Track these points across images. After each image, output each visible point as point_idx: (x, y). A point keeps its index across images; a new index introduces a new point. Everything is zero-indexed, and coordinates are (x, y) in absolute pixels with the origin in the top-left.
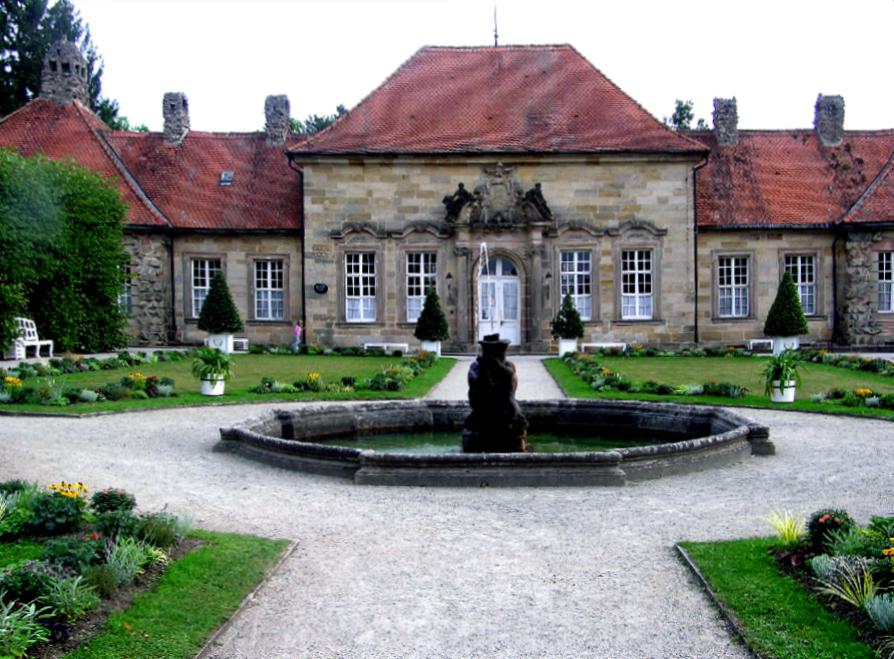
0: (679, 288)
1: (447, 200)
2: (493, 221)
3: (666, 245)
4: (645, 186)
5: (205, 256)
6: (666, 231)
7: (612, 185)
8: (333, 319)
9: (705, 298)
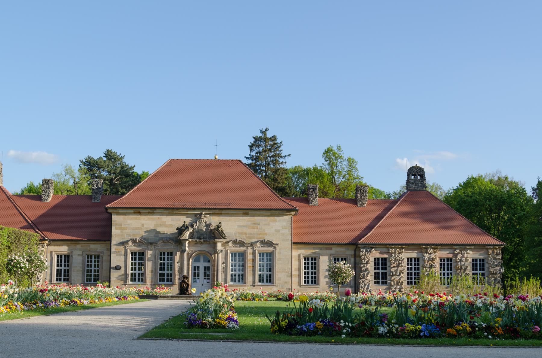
7: (255, 224)
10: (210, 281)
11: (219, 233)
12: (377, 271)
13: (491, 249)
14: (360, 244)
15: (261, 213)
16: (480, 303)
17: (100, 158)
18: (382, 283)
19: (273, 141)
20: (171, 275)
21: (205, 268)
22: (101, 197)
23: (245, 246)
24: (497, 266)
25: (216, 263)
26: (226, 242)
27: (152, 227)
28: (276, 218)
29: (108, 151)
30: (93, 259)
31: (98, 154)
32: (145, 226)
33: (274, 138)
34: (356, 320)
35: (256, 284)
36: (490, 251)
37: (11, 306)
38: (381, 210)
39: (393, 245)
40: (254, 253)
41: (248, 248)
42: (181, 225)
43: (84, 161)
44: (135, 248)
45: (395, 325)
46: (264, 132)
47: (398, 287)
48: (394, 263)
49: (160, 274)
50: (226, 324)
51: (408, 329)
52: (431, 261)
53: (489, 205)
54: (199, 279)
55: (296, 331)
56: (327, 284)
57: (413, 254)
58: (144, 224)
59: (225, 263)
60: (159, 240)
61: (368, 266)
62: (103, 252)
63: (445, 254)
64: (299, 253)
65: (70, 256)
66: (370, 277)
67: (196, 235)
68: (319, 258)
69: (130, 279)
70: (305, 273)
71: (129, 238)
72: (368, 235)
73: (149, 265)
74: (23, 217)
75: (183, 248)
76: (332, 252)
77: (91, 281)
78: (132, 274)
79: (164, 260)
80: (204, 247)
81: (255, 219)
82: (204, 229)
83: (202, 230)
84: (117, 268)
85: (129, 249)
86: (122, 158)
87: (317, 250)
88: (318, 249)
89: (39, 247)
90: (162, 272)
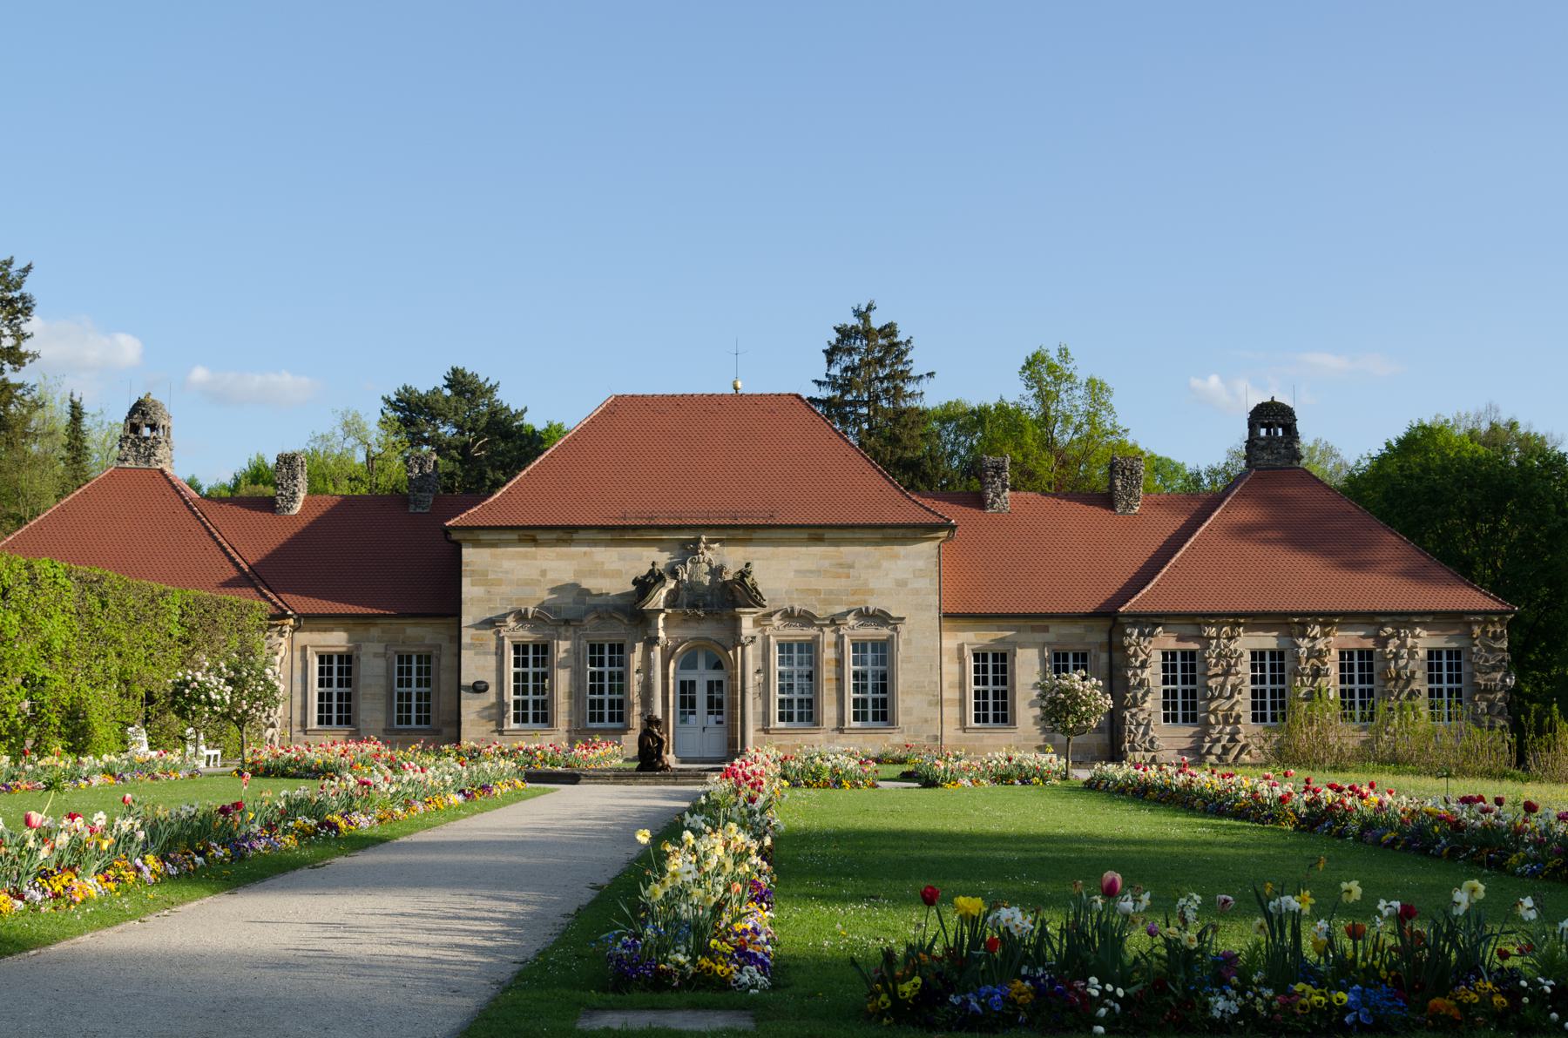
7: (841, 565)
10: (724, 718)
11: (746, 590)
12: (1170, 687)
13: (1477, 623)
14: (1123, 615)
15: (857, 536)
16: (1529, 909)
17: (436, 391)
18: (1185, 720)
19: (886, 336)
20: (621, 703)
21: (710, 684)
22: (431, 500)
23: (816, 625)
24: (1494, 668)
25: (739, 671)
26: (764, 616)
27: (568, 578)
28: (897, 549)
29: (455, 371)
30: (414, 666)
31: (429, 380)
32: (550, 576)
33: (889, 330)
34: (1137, 975)
35: (846, 726)
36: (1477, 630)
37: (123, 873)
38: (1180, 521)
39: (1212, 615)
40: (839, 644)
41: (825, 629)
42: (645, 572)
43: (394, 398)
44: (525, 635)
45: (1261, 990)
46: (863, 315)
47: (1228, 729)
48: (1216, 665)
49: (592, 702)
50: (731, 972)
51: (1304, 1001)
52: (1315, 657)
53: (1470, 501)
54: (694, 713)
55: (948, 1012)
56: (1035, 724)
57: (1268, 641)
58: (545, 570)
59: (764, 670)
60: (587, 613)
61: (1147, 674)
62: (440, 646)
63: (1352, 638)
64: (960, 642)
65: (354, 657)
66: (1153, 704)
67: (684, 595)
68: (1015, 655)
69: (512, 718)
70: (977, 693)
71: (509, 608)
72: (1144, 591)
73: (562, 680)
74: (228, 555)
75: (651, 633)
76: (1050, 636)
77: (409, 721)
78: (516, 703)
79: (601, 664)
80: (708, 630)
81: (841, 553)
82: (707, 580)
83: (700, 583)
84: (479, 688)
85: (509, 637)
86: (492, 389)
87: (1008, 633)
88: (1011, 630)
89: (271, 636)
90: (596, 697)
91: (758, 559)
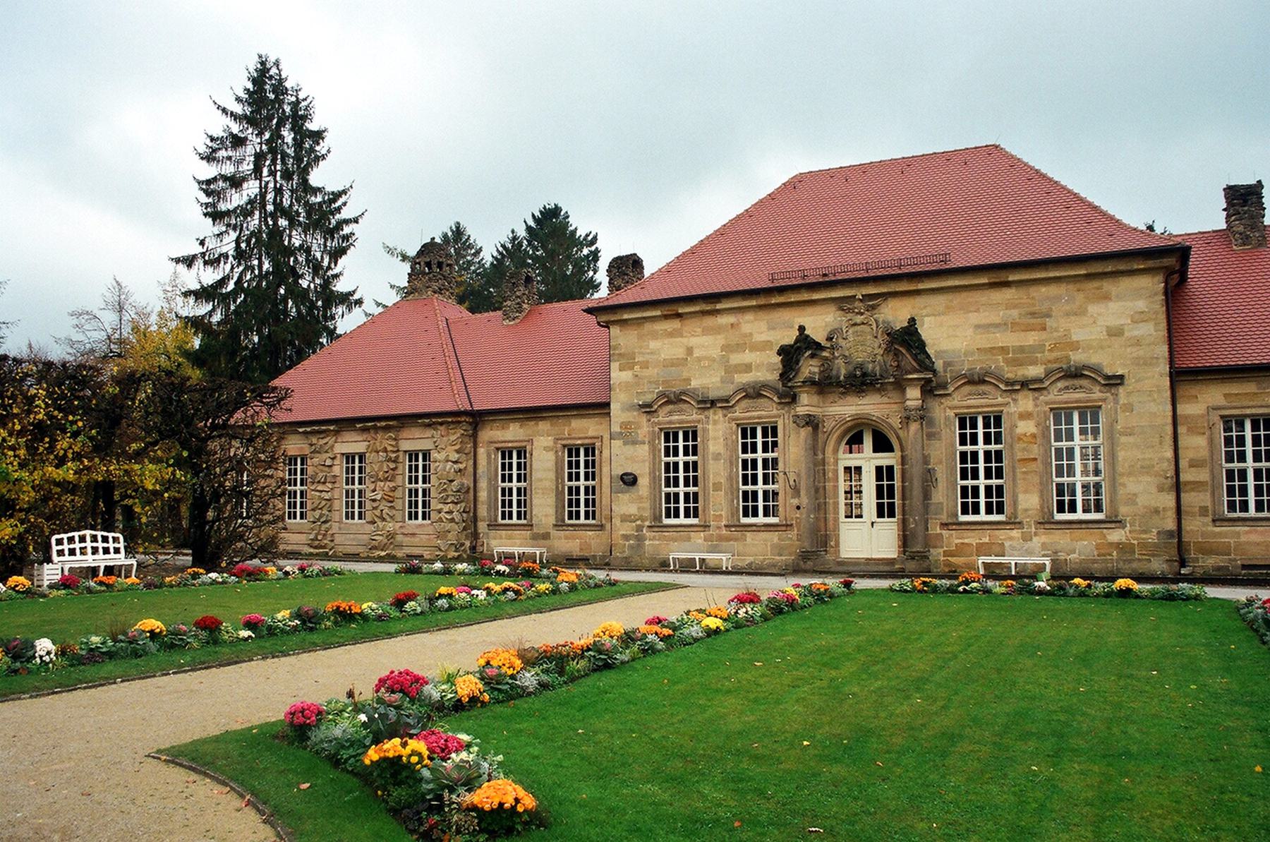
0: (1147, 469)
1: (783, 351)
2: (852, 376)
3: (1123, 400)
4: (1086, 309)
5: (510, 445)
6: (1121, 377)
7: (1033, 314)
8: (643, 519)
9: (1197, 486)
15: (1052, 274)
21: (879, 470)
91: (927, 316)
